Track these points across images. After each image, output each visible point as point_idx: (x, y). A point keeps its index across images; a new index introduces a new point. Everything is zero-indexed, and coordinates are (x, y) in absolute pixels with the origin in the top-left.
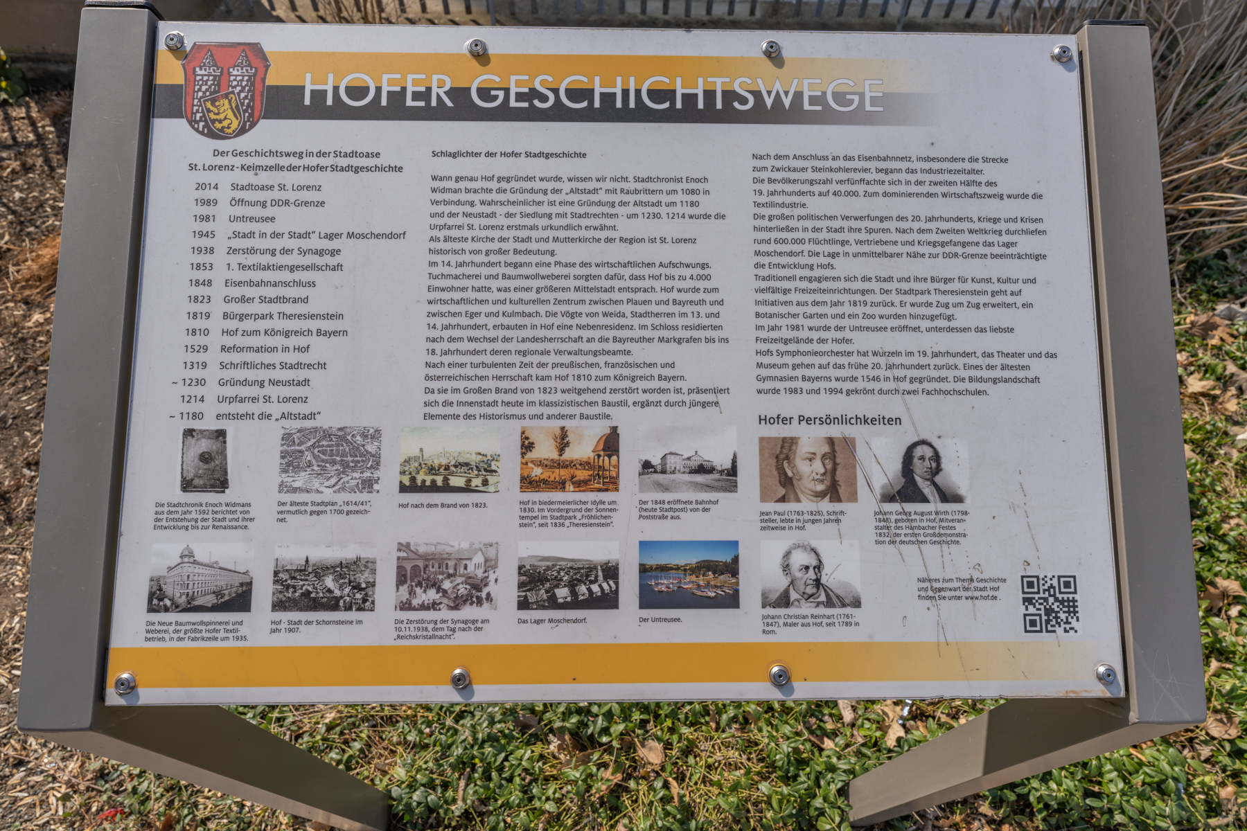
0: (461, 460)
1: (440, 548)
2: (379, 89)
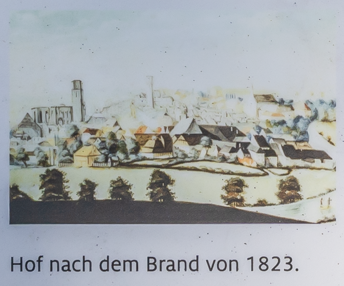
0: (209, 119)
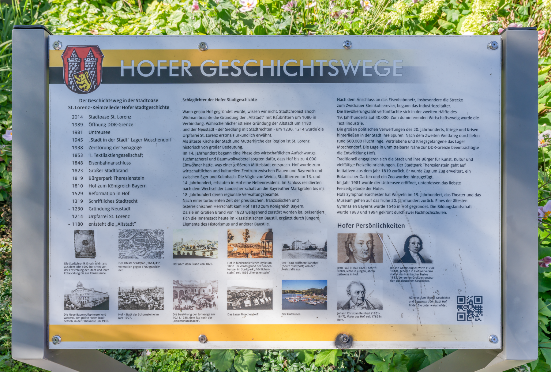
0: (200, 244)
1: (192, 283)
2: (156, 68)
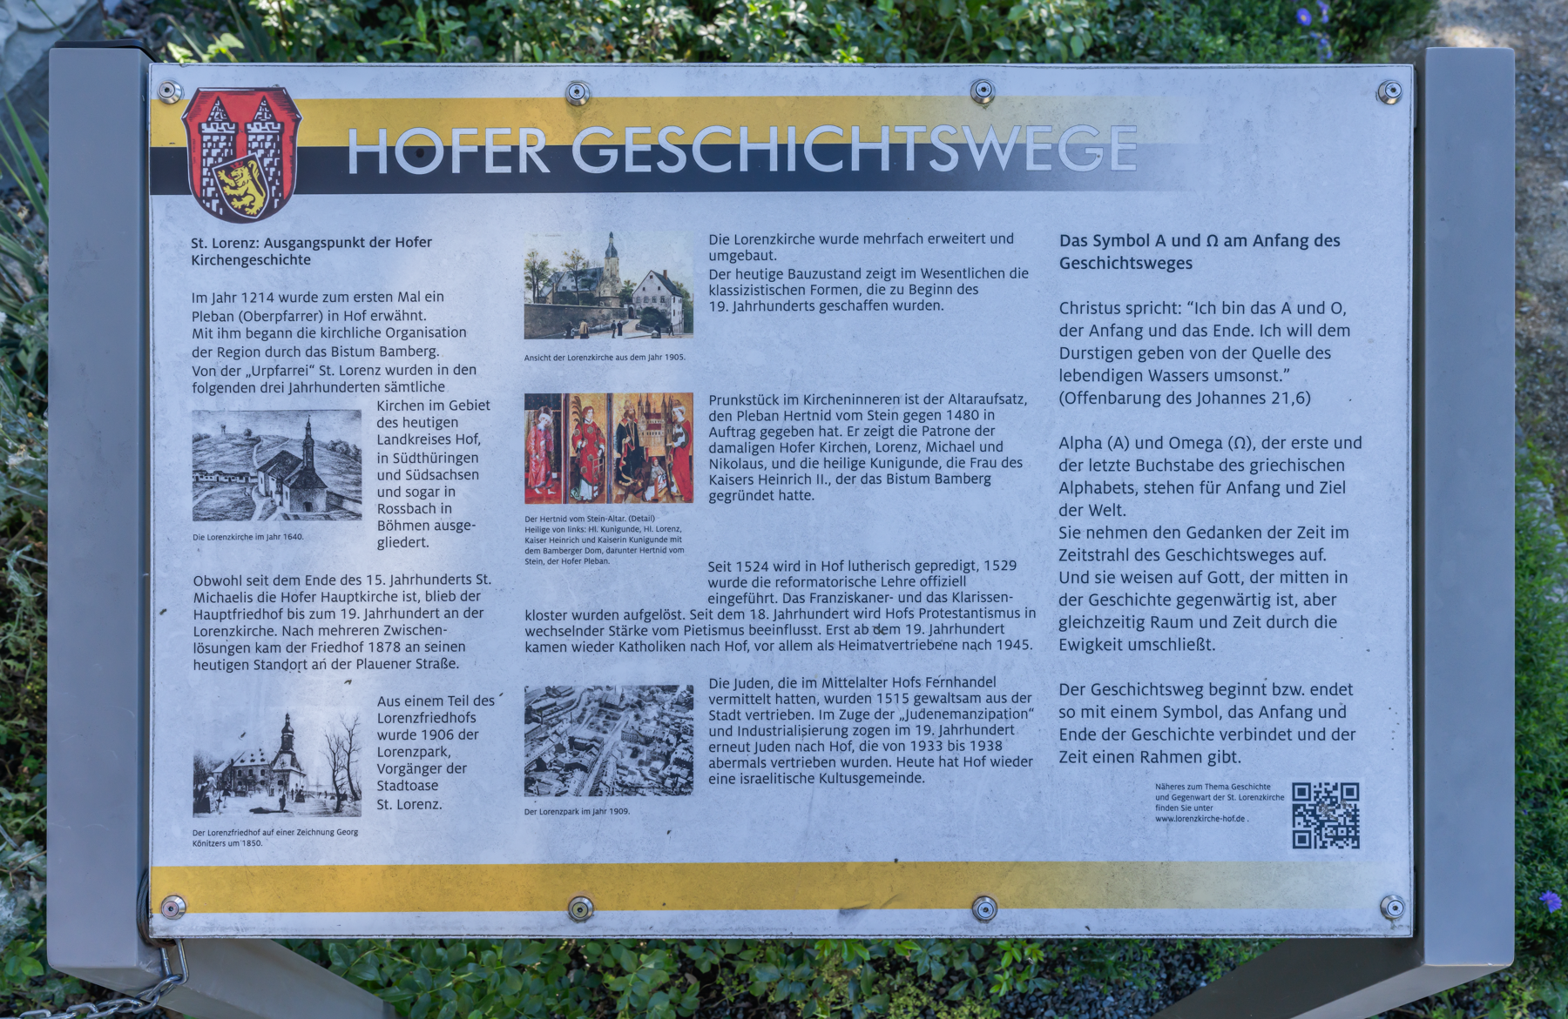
2: (448, 150)
